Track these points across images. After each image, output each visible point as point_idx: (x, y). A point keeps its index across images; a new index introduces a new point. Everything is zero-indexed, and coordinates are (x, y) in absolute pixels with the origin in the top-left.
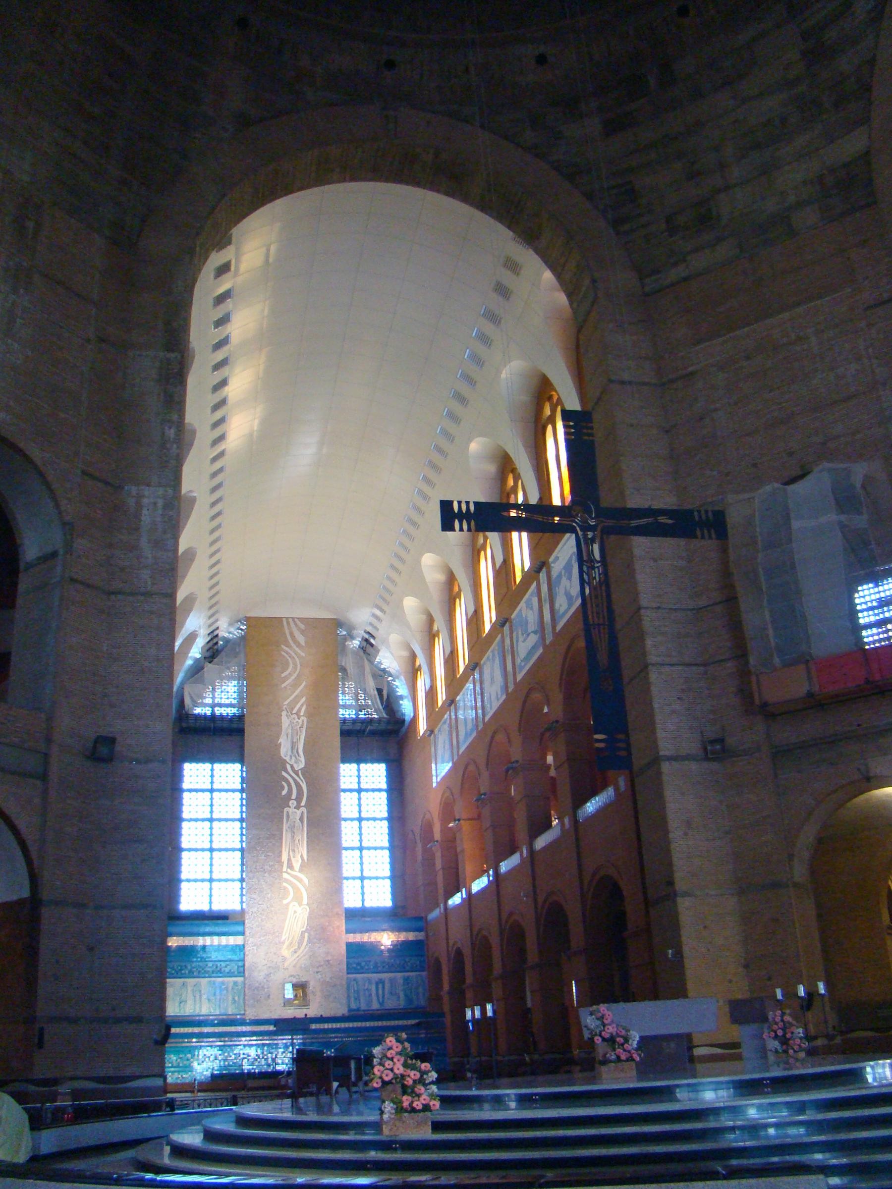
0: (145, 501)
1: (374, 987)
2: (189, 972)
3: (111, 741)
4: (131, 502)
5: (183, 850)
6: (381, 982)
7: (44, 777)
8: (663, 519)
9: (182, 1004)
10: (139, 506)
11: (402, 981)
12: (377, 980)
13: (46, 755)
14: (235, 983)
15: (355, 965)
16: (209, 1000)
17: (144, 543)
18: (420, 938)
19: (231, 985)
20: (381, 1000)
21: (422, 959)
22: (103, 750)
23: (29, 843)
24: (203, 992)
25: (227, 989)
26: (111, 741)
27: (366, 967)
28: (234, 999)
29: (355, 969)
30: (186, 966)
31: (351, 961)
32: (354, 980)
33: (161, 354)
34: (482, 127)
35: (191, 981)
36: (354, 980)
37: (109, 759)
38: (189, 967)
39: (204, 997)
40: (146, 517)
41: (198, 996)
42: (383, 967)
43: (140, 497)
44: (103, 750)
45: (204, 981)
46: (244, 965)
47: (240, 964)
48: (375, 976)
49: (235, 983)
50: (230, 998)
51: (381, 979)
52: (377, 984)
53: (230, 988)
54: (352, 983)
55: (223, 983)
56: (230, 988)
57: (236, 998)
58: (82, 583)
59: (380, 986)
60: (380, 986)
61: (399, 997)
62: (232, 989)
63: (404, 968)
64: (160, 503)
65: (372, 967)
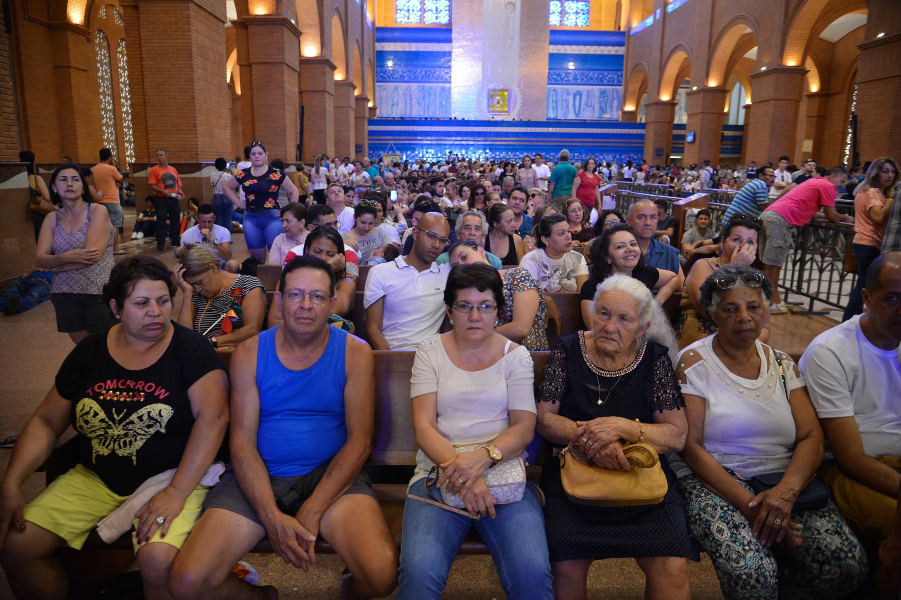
1: (571, 98)
2: (400, 77)
6: (579, 94)
9: (394, 107)
11: (598, 94)
12: (575, 91)
15: (555, 77)
16: (419, 104)
18: (620, 53)
19: (439, 89)
20: (577, 112)
21: (619, 74)
24: (413, 96)
27: (566, 79)
28: (441, 103)
29: (556, 80)
31: (552, 72)
32: (554, 90)
36: (554, 90)
38: (400, 73)
39: (414, 100)
42: (582, 79)
45: (414, 86)
48: (573, 88)
50: (438, 103)
51: (579, 92)
52: (575, 95)
53: (438, 93)
54: (552, 93)
56: (438, 93)
57: (444, 103)
59: (578, 97)
60: (578, 97)
61: (594, 109)
62: (441, 94)
63: (602, 81)
65: (571, 79)
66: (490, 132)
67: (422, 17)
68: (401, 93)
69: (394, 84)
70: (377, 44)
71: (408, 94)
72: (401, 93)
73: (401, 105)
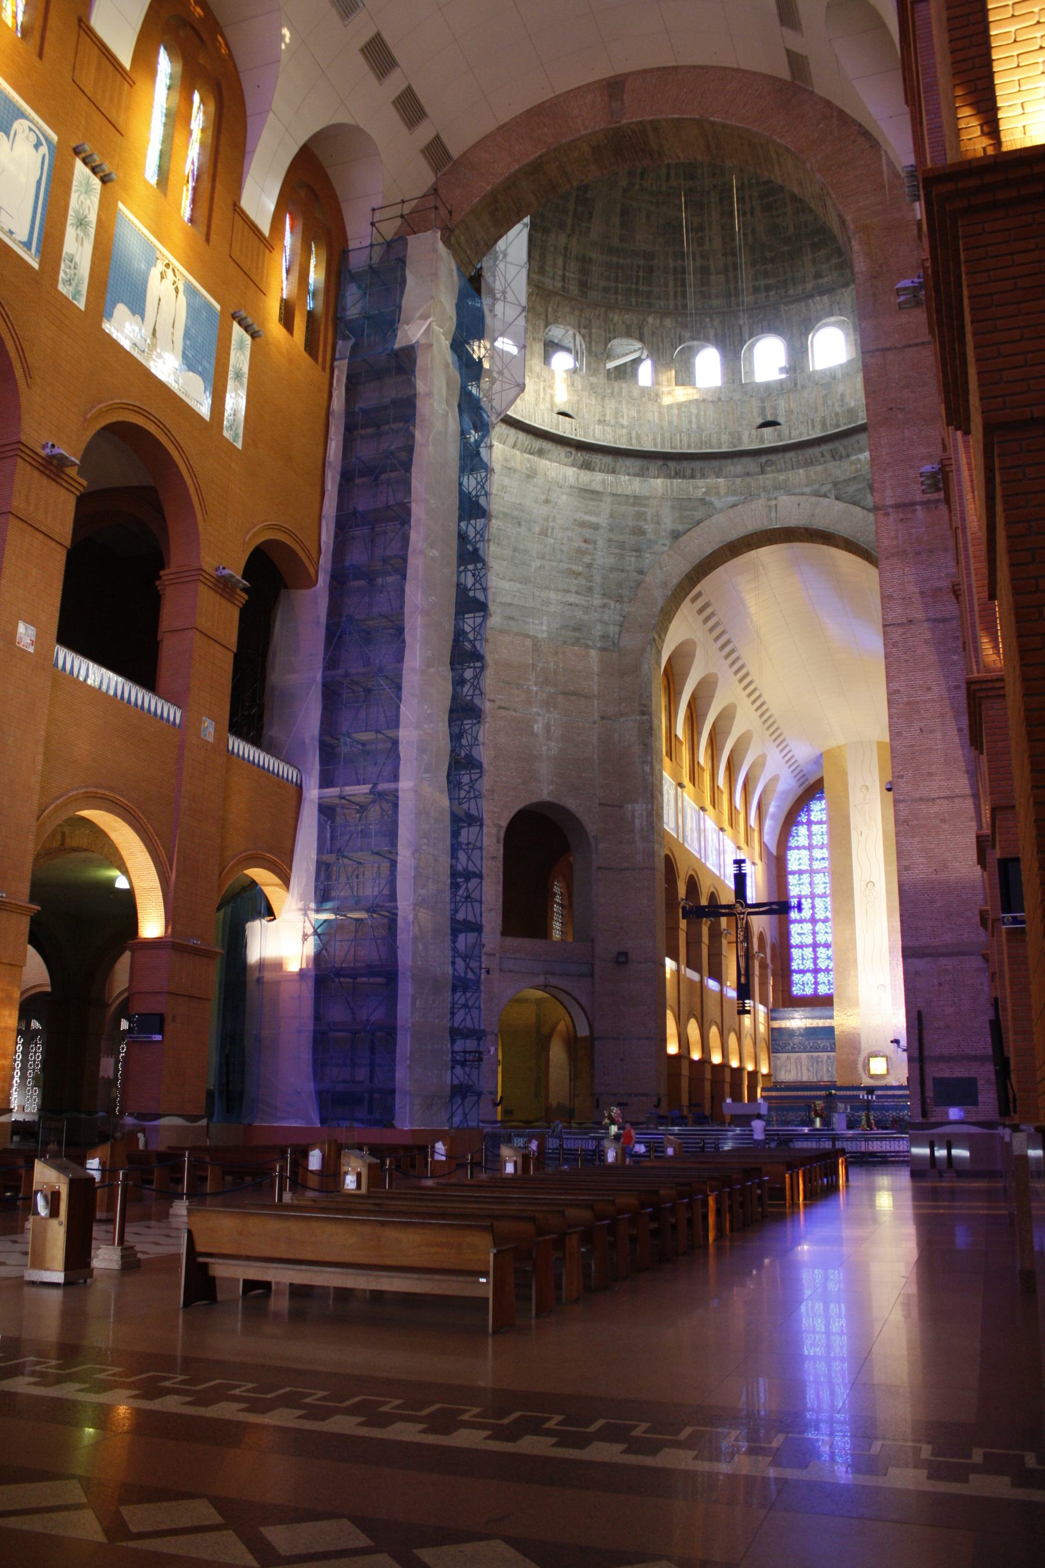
0: (637, 813)
3: (625, 954)
4: (629, 815)
5: (792, 946)
7: (592, 975)
8: (774, 907)
10: (633, 816)
13: (592, 965)
14: (829, 1057)
16: (808, 1070)
17: (637, 838)
19: (825, 1060)
22: (622, 959)
23: (587, 1010)
25: (822, 1061)
26: (625, 954)
30: (789, 1044)
33: (638, 718)
34: (837, 498)
35: (794, 1056)
37: (626, 963)
39: (804, 1068)
40: (637, 822)
41: (799, 1068)
43: (634, 811)
44: (622, 959)
45: (804, 1055)
46: (834, 1044)
47: (832, 1042)
49: (829, 1057)
50: (825, 1069)
53: (825, 1060)
55: (818, 1057)
58: (605, 868)
64: (645, 813)
66: (817, 1091)
67: (816, 989)
68: (793, 1061)
69: (787, 1054)
70: (771, 1022)
71: (798, 1061)
72: (793, 1061)
73: (793, 1072)
